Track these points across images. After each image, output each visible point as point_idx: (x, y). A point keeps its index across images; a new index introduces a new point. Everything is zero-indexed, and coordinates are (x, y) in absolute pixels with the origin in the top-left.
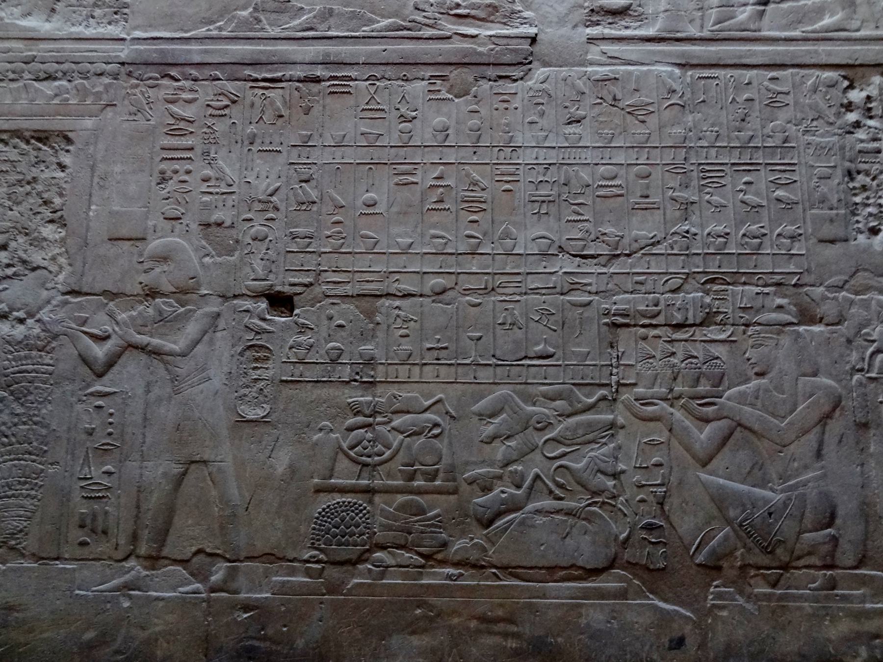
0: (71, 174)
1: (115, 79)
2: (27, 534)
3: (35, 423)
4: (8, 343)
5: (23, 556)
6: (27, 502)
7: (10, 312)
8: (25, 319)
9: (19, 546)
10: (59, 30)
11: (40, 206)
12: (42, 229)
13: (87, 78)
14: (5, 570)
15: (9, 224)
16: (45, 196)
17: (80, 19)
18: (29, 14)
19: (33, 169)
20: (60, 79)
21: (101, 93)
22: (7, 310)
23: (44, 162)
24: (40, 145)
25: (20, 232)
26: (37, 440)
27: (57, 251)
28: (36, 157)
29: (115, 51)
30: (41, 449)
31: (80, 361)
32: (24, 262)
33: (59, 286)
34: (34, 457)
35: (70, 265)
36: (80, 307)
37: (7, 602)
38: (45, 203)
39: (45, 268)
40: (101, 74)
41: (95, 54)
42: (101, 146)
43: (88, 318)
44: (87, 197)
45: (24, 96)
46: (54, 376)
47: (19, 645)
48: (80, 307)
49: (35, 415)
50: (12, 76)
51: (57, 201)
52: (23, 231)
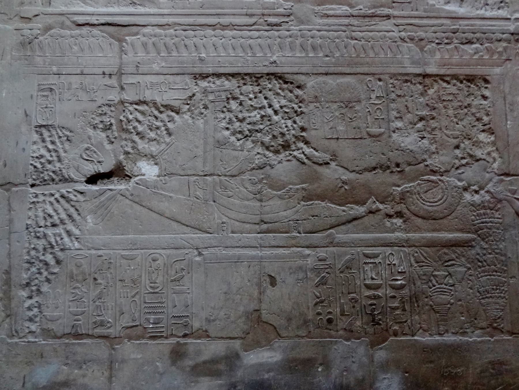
0: (492, 102)
1: (509, 43)
2: (503, 320)
3: (497, 254)
4: (472, 205)
5: (502, 332)
6: (500, 301)
7: (469, 187)
8: (478, 191)
9: (499, 327)
10: (469, 12)
11: (475, 121)
12: (479, 136)
13: (492, 43)
14: (494, 341)
15: (458, 133)
16: (478, 115)
17: (481, 6)
18: (449, 2)
19: (467, 99)
20: (475, 43)
21: (502, 52)
22: (466, 185)
23: (473, 94)
24: (469, 84)
25: (465, 138)
26: (499, 263)
27: (490, 149)
28: (468, 91)
29: (505, 26)
30: (503, 269)
31: (515, 215)
32: (471, 156)
33: (495, 170)
34: (499, 274)
35: (500, 157)
36: (511, 183)
37: (498, 360)
38: (478, 120)
39: (484, 160)
40: (500, 41)
41: (495, 28)
42: (507, 84)
43: (516, 190)
44: (504, 116)
45: (456, 53)
46: (502, 225)
47: (510, 385)
48: (511, 183)
49: (496, 249)
50: (446, 41)
51: (486, 119)
52: (467, 137)
